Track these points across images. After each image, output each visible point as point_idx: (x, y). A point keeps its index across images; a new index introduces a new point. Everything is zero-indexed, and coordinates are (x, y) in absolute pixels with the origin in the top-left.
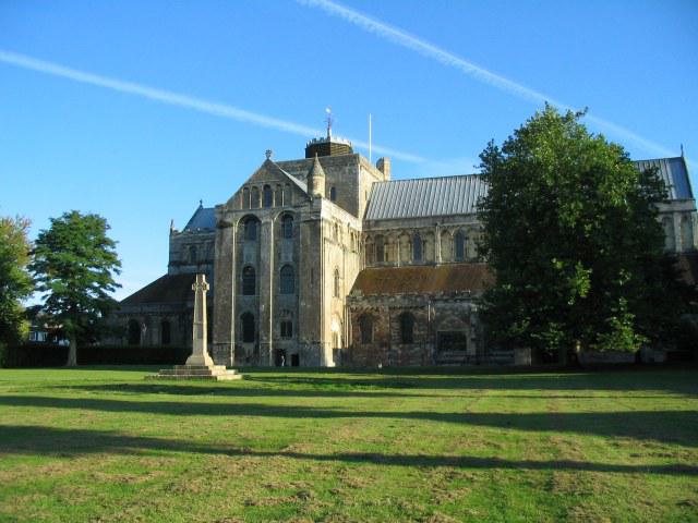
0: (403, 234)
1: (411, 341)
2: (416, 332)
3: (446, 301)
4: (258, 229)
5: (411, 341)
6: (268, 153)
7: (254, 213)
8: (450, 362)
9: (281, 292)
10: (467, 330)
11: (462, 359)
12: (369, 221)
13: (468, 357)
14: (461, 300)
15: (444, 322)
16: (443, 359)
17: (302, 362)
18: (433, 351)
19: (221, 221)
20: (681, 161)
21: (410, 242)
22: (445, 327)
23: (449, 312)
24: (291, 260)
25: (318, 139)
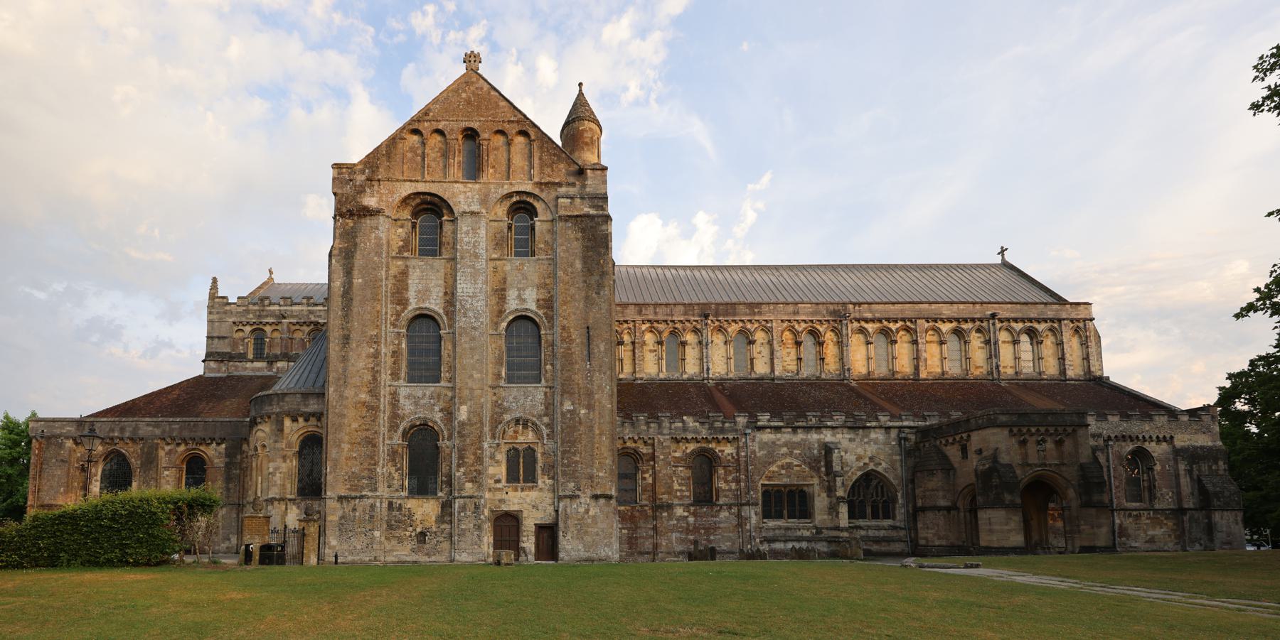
4: (447, 228)
7: (434, 189)
14: (808, 429)
23: (784, 450)
24: (532, 306)
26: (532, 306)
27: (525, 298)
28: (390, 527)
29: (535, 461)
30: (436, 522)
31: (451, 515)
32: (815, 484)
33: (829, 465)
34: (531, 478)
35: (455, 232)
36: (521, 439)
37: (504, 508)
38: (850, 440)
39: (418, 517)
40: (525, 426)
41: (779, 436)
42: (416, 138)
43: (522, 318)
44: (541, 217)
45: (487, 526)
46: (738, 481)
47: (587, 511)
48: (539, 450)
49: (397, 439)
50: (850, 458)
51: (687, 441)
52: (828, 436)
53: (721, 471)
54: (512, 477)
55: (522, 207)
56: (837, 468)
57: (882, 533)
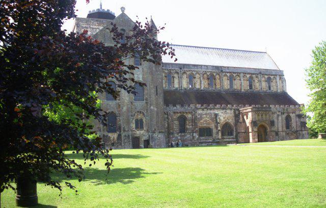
3: (203, 109)
5: (184, 132)
11: (211, 141)
14: (211, 109)
15: (202, 121)
16: (202, 141)
18: (197, 137)
21: (166, 77)
22: (202, 123)
23: (205, 116)
29: (143, 122)
30: (117, 140)
31: (121, 138)
32: (213, 126)
33: (216, 120)
34: (142, 128)
36: (139, 117)
39: (112, 139)
42: (108, 30)
46: (192, 125)
50: (222, 118)
53: (187, 122)
54: (137, 127)
56: (218, 120)
57: (230, 140)
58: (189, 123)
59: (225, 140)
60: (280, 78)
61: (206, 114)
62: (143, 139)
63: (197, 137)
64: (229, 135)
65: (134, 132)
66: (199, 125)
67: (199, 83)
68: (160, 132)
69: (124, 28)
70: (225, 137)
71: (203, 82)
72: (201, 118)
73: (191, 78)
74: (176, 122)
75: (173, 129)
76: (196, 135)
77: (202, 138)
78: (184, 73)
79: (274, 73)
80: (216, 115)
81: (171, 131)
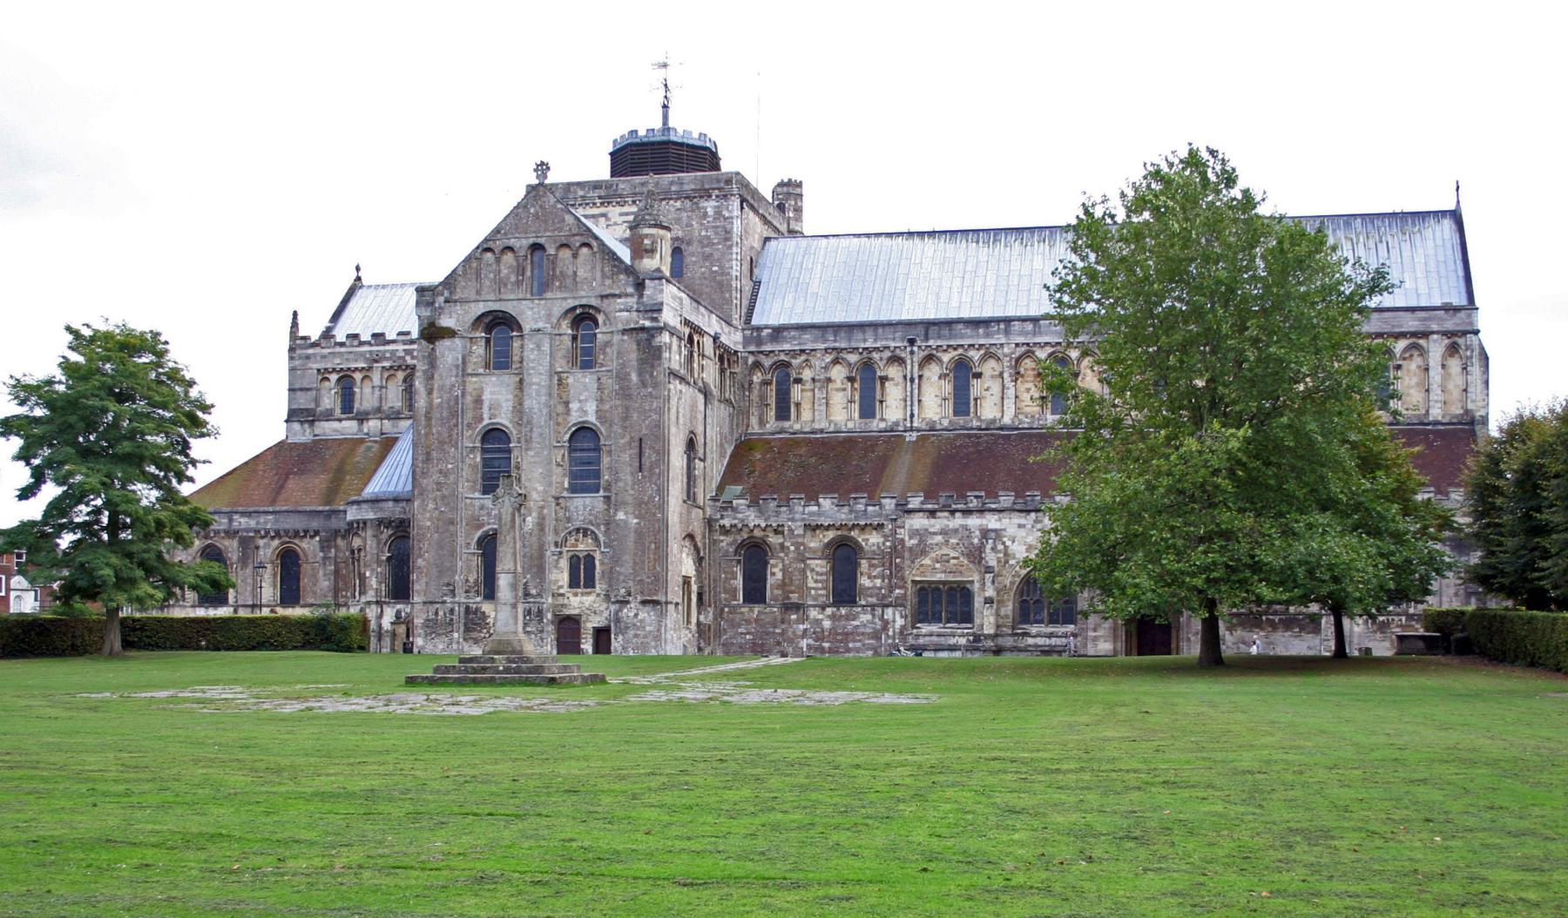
0: (836, 362)
1: (852, 602)
2: (864, 581)
3: (932, 513)
4: (516, 344)
5: (852, 602)
6: (542, 168)
8: (938, 648)
9: (574, 489)
10: (976, 577)
11: (963, 641)
12: (759, 329)
13: (977, 638)
14: (967, 512)
15: (927, 561)
16: (921, 641)
17: (616, 644)
18: (900, 622)
19: (432, 324)
20: (1456, 216)
21: (851, 379)
22: (928, 569)
23: (939, 538)
25: (642, 133)
26: (592, 418)
27: (585, 410)
28: (467, 630)
34: (590, 583)
35: (522, 346)
36: (581, 547)
37: (567, 612)
38: (1020, 526)
40: (585, 535)
41: (933, 521)
42: (489, 255)
43: (583, 432)
44: (602, 329)
45: (551, 628)
47: (636, 615)
48: (598, 556)
49: (473, 548)
51: (828, 528)
52: (992, 522)
54: (574, 583)
55: (583, 318)
58: (871, 566)
59: (1030, 641)
60: (1453, 349)
61: (944, 532)
62: (590, 625)
63: (900, 622)
64: (1053, 620)
65: (561, 601)
66: (913, 575)
67: (997, 398)
68: (644, 602)
69: (541, 241)
70: (1034, 630)
71: (1011, 392)
72: (922, 550)
73: (963, 373)
74: (820, 566)
75: (803, 588)
76: (897, 619)
77: (925, 628)
78: (929, 358)
79: (1411, 323)
80: (985, 533)
81: (794, 597)
